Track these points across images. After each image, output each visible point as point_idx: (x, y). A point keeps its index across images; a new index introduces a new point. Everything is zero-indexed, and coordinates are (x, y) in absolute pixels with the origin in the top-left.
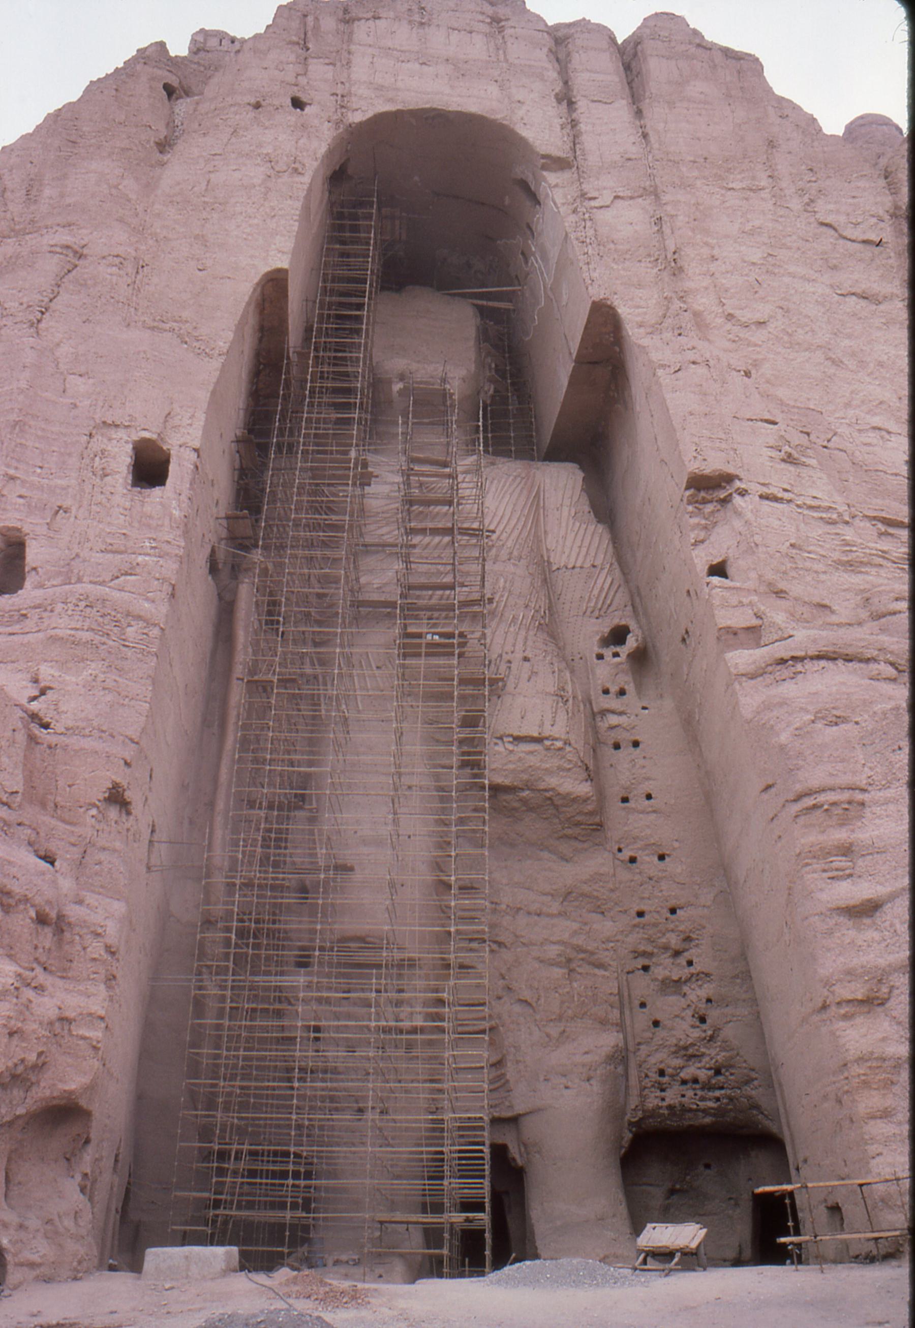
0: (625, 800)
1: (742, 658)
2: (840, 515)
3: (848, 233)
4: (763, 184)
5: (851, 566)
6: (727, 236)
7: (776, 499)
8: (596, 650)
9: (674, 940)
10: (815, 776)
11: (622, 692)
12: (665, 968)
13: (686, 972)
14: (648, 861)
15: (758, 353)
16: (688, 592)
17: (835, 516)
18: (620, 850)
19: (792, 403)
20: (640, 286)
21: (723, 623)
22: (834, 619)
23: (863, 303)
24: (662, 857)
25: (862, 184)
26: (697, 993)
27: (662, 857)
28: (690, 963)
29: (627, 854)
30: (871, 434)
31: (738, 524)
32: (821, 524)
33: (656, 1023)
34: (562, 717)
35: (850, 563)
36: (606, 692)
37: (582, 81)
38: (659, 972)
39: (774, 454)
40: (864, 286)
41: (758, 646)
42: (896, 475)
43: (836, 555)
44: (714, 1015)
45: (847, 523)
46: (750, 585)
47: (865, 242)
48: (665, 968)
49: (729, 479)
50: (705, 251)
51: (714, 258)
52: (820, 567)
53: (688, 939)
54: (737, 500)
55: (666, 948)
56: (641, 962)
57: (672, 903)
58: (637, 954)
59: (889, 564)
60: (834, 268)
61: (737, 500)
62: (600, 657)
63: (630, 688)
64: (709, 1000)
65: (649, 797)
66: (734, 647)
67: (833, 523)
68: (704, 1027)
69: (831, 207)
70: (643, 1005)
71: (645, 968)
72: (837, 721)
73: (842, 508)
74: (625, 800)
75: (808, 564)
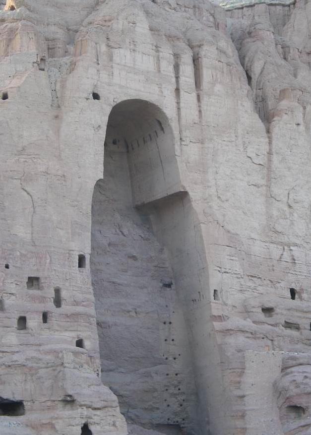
1: (217, 325)
2: (241, 275)
4: (233, 140)
6: (221, 163)
7: (227, 273)
9: (176, 383)
12: (172, 390)
13: (176, 392)
15: (225, 211)
16: (199, 292)
17: (240, 276)
18: (164, 355)
20: (196, 184)
21: (214, 314)
23: (255, 187)
25: (262, 140)
32: (236, 279)
33: (168, 406)
35: (241, 291)
38: (171, 391)
40: (256, 182)
42: (255, 256)
43: (239, 289)
44: (185, 404)
45: (242, 278)
47: (260, 164)
48: (172, 390)
50: (215, 169)
51: (217, 173)
52: (235, 293)
53: (179, 383)
55: (173, 385)
56: (166, 388)
57: (176, 373)
58: (165, 386)
59: (250, 290)
60: (249, 175)
64: (184, 400)
65: (173, 340)
66: (215, 321)
67: (239, 278)
68: (181, 407)
70: (165, 400)
71: (167, 390)
75: (233, 293)
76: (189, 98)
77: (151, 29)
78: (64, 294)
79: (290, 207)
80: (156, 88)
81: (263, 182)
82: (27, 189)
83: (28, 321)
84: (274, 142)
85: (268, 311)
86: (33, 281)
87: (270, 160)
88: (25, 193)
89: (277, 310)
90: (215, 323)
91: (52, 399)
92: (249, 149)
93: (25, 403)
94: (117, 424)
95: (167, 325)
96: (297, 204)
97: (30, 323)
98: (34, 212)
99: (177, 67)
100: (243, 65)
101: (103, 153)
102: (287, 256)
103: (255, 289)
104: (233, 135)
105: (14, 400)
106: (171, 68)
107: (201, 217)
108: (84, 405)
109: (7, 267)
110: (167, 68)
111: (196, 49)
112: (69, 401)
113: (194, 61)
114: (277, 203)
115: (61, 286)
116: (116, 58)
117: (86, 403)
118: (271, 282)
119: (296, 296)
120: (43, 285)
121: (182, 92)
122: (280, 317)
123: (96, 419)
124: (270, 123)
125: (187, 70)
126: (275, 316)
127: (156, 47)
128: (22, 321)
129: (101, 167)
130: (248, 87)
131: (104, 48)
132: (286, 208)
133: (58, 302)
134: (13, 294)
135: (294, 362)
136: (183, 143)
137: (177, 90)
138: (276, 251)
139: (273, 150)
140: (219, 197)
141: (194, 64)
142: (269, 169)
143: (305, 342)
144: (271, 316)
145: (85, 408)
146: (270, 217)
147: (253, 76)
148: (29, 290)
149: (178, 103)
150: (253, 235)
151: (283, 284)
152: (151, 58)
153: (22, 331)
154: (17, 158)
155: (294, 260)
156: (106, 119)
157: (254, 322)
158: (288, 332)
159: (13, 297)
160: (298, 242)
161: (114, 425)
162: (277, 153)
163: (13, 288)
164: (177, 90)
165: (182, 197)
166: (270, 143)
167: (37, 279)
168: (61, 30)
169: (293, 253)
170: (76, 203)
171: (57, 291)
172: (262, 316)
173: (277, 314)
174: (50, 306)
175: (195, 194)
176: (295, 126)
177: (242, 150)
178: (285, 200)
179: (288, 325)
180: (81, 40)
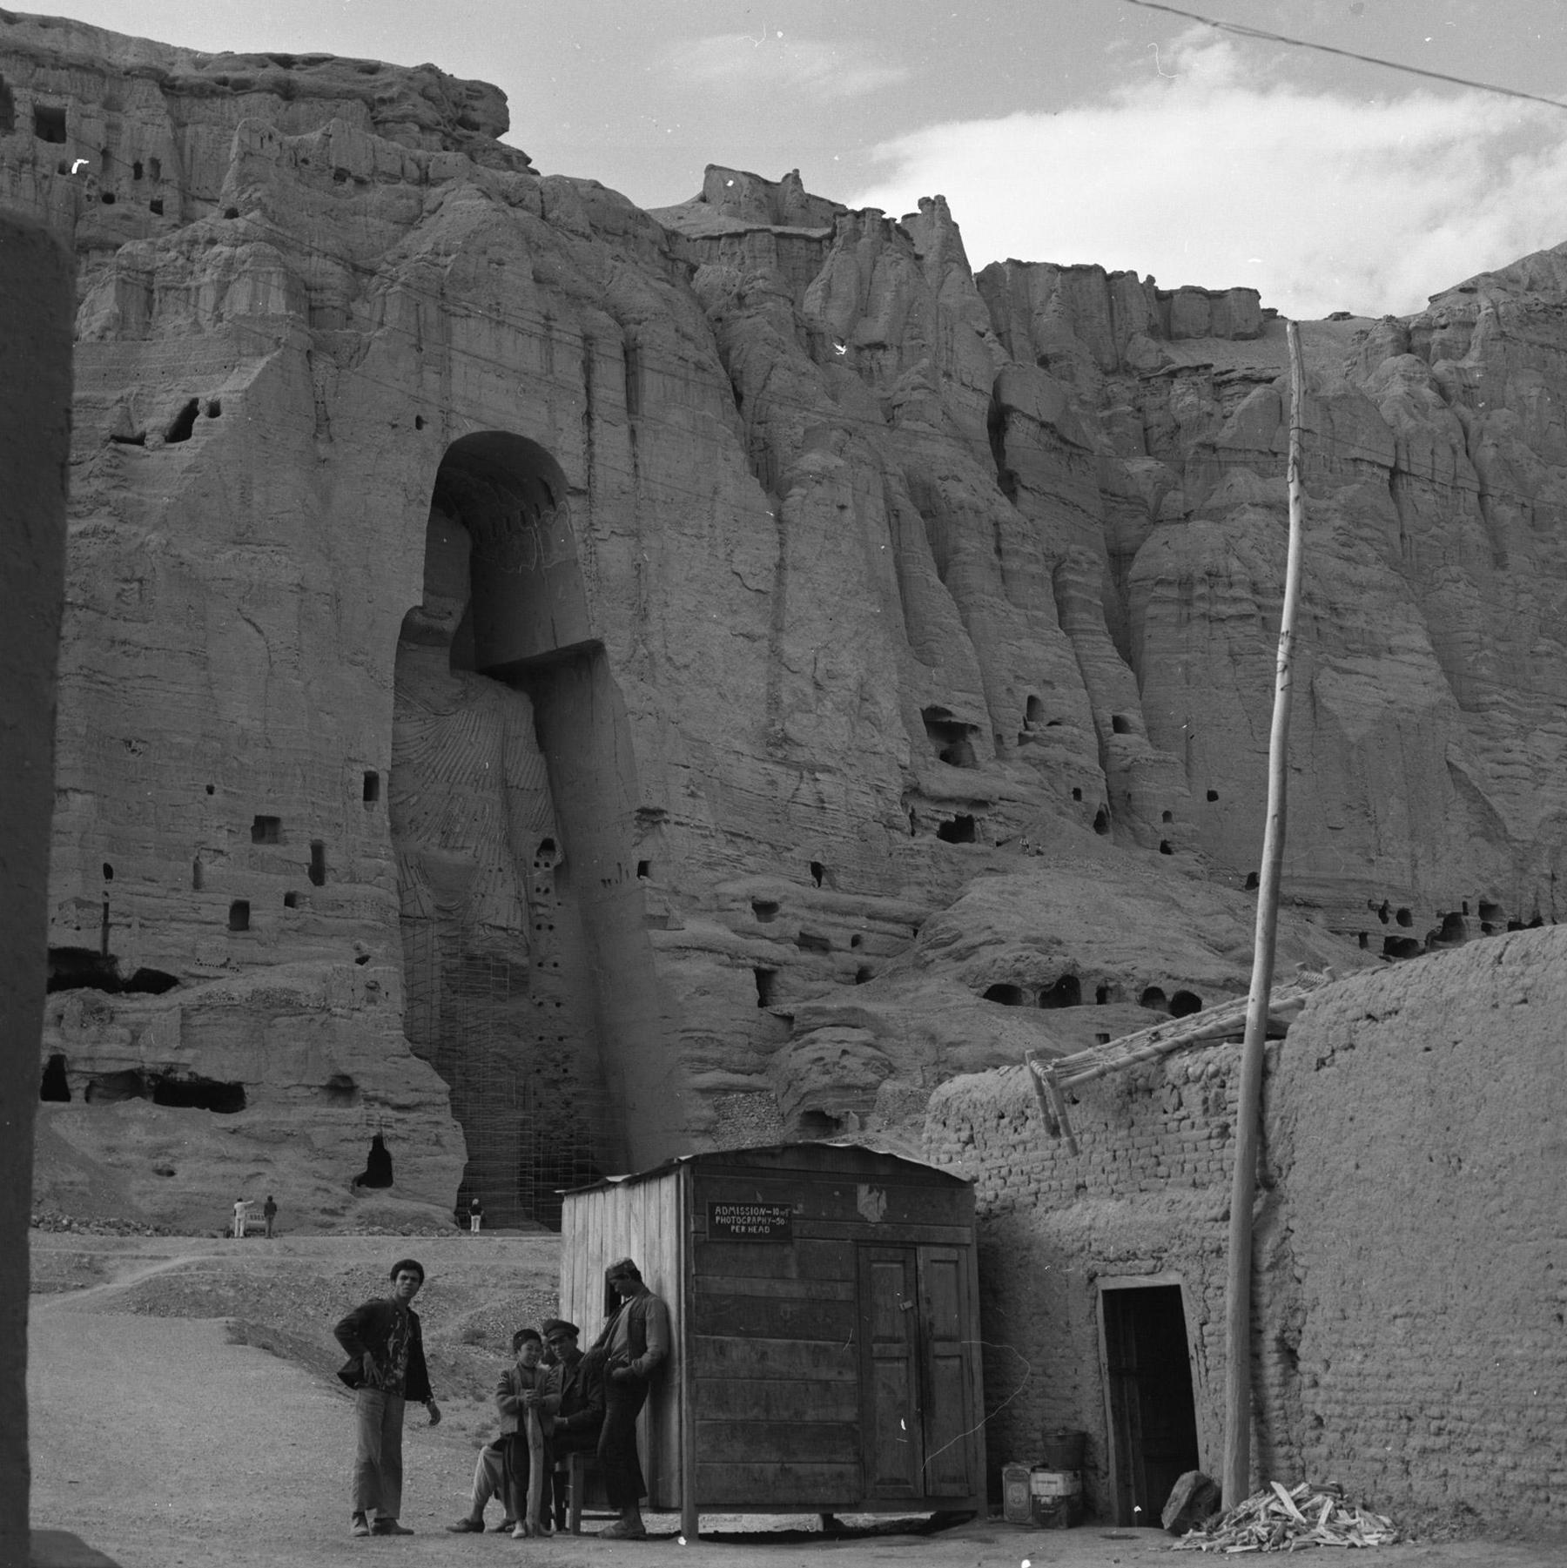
0: (540, 965)
1: (660, 937)
3: (750, 583)
5: (710, 865)
7: (682, 824)
8: (535, 859)
9: (559, 1056)
10: (694, 1022)
11: (547, 891)
14: (550, 1008)
19: (696, 735)
22: (699, 906)
24: (558, 1005)
25: (764, 536)
26: (568, 1090)
27: (558, 1005)
28: (565, 1071)
29: (538, 1000)
30: (733, 756)
31: (661, 841)
34: (519, 914)
36: (538, 890)
37: (600, 409)
39: (683, 790)
41: (665, 929)
43: (704, 859)
46: (663, 886)
49: (662, 812)
51: (666, 605)
54: (664, 826)
60: (735, 612)
61: (664, 826)
62: (537, 865)
63: (552, 889)
67: (705, 837)
69: (742, 557)
71: (538, 1071)
72: (706, 993)
73: (712, 827)
74: (540, 965)
76: (611, 439)
77: (537, 280)
78: (331, 858)
79: (818, 686)
80: (544, 410)
81: (763, 629)
82: (258, 621)
83: (252, 913)
84: (790, 544)
85: (765, 909)
86: (265, 828)
87: (780, 582)
88: (251, 630)
89: (784, 908)
90: (652, 932)
91: (304, 1082)
92: (738, 556)
93: (247, 1089)
94: (445, 1140)
95: (545, 931)
96: (834, 682)
97: (255, 917)
98: (271, 674)
99: (588, 368)
100: (726, 367)
101: (424, 547)
102: (807, 792)
103: (738, 860)
104: (706, 524)
105: (222, 1080)
106: (577, 366)
107: (631, 702)
108: (375, 1099)
109: (210, 790)
110: (569, 368)
111: (633, 328)
112: (342, 1088)
113: (626, 353)
114: (792, 677)
115: (325, 840)
116: (459, 341)
117: (381, 1094)
118: (772, 846)
119: (824, 879)
120: (288, 834)
121: (597, 422)
122: (791, 923)
123: (400, 1129)
124: (783, 500)
125: (610, 375)
126: (779, 920)
127: (547, 318)
128: (240, 913)
129: (420, 581)
130: (736, 416)
131: (433, 314)
132: (809, 690)
133: (317, 873)
134: (221, 852)
135: (822, 1020)
136: (598, 535)
137: (588, 417)
138: (787, 781)
139: (788, 561)
140: (669, 659)
141: (627, 361)
142: (779, 601)
143: (841, 977)
144: (770, 920)
145: (377, 1105)
146: (774, 703)
147: (745, 391)
148: (256, 847)
149: (590, 443)
150: (738, 745)
151: (796, 853)
152: (535, 343)
153: (240, 934)
154: (236, 550)
155: (822, 801)
156: (432, 473)
157: (735, 931)
158: (807, 957)
159: (222, 860)
160: (831, 763)
161: (438, 1142)
162: (795, 569)
163: (222, 840)
164: (588, 417)
165: (588, 655)
166: (782, 544)
167: (274, 821)
168: (339, 269)
169: (820, 786)
170: (360, 658)
171: (318, 850)
172: (749, 919)
173: (784, 916)
174: (301, 883)
175: (616, 650)
176: (836, 511)
177: (722, 557)
178: (809, 670)
179: (807, 942)
180: (384, 295)
